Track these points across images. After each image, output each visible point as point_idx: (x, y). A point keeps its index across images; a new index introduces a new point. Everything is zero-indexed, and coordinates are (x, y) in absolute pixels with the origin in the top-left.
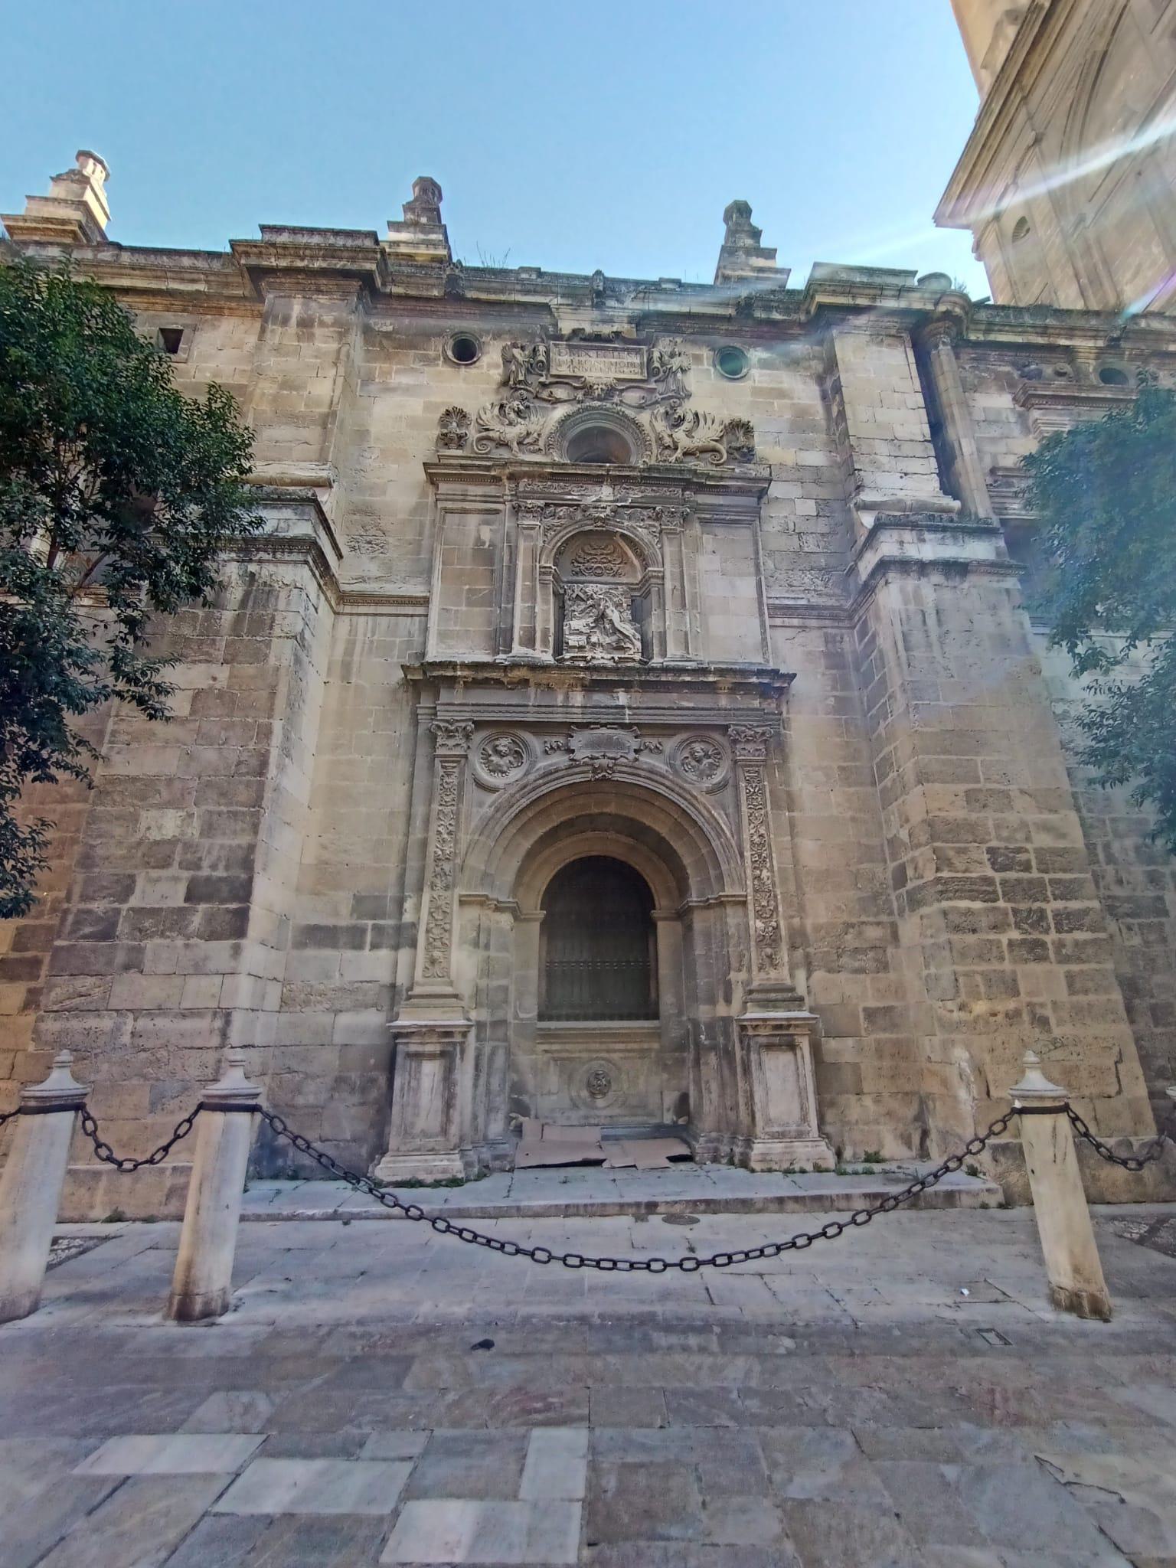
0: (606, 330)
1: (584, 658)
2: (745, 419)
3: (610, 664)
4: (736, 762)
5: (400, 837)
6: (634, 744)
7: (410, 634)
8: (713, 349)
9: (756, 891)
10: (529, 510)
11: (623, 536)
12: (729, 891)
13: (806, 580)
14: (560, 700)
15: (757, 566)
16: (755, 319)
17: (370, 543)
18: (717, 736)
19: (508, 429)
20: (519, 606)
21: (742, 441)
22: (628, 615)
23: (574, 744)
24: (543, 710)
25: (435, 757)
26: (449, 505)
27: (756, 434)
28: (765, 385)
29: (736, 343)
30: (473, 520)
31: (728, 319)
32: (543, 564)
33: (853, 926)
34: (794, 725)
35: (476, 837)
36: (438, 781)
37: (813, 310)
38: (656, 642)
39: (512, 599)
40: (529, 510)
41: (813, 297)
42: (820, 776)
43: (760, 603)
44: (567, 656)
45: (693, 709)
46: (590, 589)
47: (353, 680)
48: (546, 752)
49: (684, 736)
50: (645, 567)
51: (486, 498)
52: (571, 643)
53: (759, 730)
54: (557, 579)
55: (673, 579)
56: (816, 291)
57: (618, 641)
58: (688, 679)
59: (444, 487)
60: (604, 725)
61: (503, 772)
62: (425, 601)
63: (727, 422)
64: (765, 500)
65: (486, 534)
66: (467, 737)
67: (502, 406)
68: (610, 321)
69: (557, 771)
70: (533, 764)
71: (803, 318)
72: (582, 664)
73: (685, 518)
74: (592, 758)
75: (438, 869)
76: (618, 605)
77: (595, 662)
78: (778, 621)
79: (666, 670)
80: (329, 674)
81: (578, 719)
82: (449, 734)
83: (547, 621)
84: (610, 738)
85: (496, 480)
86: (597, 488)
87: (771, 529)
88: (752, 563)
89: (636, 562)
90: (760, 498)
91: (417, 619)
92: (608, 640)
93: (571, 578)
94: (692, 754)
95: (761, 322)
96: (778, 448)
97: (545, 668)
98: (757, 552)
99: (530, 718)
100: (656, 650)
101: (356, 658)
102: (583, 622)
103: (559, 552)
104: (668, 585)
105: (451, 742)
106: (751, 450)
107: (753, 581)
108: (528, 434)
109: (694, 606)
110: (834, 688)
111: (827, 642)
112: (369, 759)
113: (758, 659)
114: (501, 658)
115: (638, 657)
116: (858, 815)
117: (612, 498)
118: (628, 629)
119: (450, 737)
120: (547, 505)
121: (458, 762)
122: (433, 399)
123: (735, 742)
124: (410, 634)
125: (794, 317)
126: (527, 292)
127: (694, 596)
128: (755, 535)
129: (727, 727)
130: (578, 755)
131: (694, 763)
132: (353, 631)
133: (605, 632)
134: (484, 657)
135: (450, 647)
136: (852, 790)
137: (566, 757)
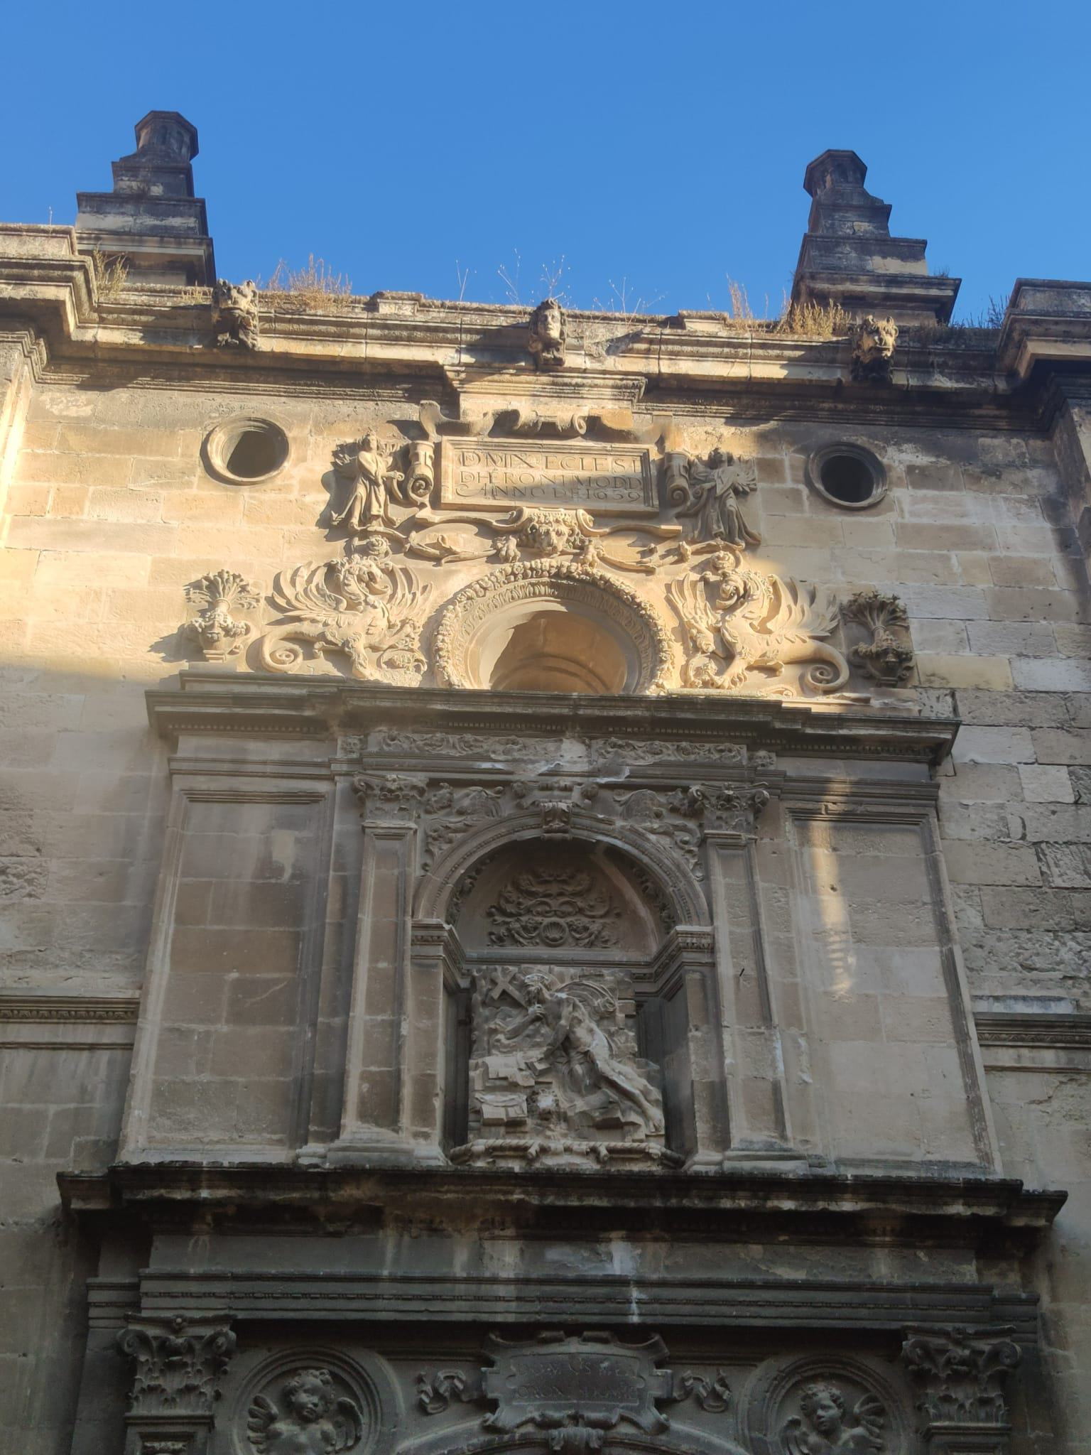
0: (564, 412)
1: (521, 1152)
2: (886, 593)
3: (588, 1166)
4: (928, 1436)
6: (654, 1381)
7: (83, 1093)
8: (804, 450)
10: (390, 796)
11: (614, 853)
13: (1065, 954)
14: (460, 1263)
15: (942, 923)
16: (899, 388)
18: (874, 1363)
19: (346, 618)
20: (360, 1015)
21: (883, 638)
22: (628, 1039)
23: (497, 1382)
24: (416, 1289)
25: (127, 1423)
26: (202, 783)
27: (914, 624)
28: (925, 520)
29: (858, 437)
30: (255, 819)
31: (835, 391)
32: (422, 917)
34: (1074, 1332)
37: (1023, 370)
38: (701, 1109)
39: (344, 1005)
40: (390, 796)
41: (1021, 346)
43: (957, 1011)
44: (479, 1145)
46: (535, 977)
48: (422, 1409)
49: (785, 1362)
50: (667, 922)
51: (288, 770)
52: (489, 1112)
53: (985, 1346)
54: (455, 955)
55: (735, 954)
56: (1026, 334)
57: (608, 1106)
58: (788, 1205)
59: (189, 746)
60: (575, 1330)
62: (129, 1012)
63: (845, 599)
64: (946, 767)
65: (286, 849)
66: (216, 1366)
67: (331, 570)
68: (574, 391)
71: (1002, 385)
72: (517, 1166)
73: (758, 809)
74: (546, 1424)
76: (604, 1017)
77: (550, 1162)
78: (1006, 1057)
81: (506, 1313)
82: (170, 1360)
83: (429, 1056)
84: (592, 1364)
85: (314, 729)
86: (551, 746)
87: (966, 834)
88: (927, 915)
89: (643, 912)
90: (935, 763)
91: (104, 1056)
92: (581, 1104)
93: (486, 951)
95: (906, 395)
96: (967, 653)
97: (426, 1177)
98: (936, 887)
99: (385, 1311)
100: (702, 1128)
102: (518, 1058)
103: (461, 891)
104: (726, 968)
105: (171, 1383)
106: (904, 658)
107: (931, 958)
109: (794, 1019)
113: (965, 1153)
114: (312, 1153)
115: (656, 1147)
117: (585, 767)
118: (630, 1076)
119: (171, 1367)
120: (434, 784)
121: (188, 1438)
122: (173, 555)
123: (922, 1378)
124: (83, 1093)
125: (985, 383)
126: (396, 341)
128: (929, 848)
129: (897, 1337)
130: (506, 1416)
131: (813, 1438)
133: (574, 1084)
134: (277, 1155)
135: (185, 1126)
137: (475, 1423)
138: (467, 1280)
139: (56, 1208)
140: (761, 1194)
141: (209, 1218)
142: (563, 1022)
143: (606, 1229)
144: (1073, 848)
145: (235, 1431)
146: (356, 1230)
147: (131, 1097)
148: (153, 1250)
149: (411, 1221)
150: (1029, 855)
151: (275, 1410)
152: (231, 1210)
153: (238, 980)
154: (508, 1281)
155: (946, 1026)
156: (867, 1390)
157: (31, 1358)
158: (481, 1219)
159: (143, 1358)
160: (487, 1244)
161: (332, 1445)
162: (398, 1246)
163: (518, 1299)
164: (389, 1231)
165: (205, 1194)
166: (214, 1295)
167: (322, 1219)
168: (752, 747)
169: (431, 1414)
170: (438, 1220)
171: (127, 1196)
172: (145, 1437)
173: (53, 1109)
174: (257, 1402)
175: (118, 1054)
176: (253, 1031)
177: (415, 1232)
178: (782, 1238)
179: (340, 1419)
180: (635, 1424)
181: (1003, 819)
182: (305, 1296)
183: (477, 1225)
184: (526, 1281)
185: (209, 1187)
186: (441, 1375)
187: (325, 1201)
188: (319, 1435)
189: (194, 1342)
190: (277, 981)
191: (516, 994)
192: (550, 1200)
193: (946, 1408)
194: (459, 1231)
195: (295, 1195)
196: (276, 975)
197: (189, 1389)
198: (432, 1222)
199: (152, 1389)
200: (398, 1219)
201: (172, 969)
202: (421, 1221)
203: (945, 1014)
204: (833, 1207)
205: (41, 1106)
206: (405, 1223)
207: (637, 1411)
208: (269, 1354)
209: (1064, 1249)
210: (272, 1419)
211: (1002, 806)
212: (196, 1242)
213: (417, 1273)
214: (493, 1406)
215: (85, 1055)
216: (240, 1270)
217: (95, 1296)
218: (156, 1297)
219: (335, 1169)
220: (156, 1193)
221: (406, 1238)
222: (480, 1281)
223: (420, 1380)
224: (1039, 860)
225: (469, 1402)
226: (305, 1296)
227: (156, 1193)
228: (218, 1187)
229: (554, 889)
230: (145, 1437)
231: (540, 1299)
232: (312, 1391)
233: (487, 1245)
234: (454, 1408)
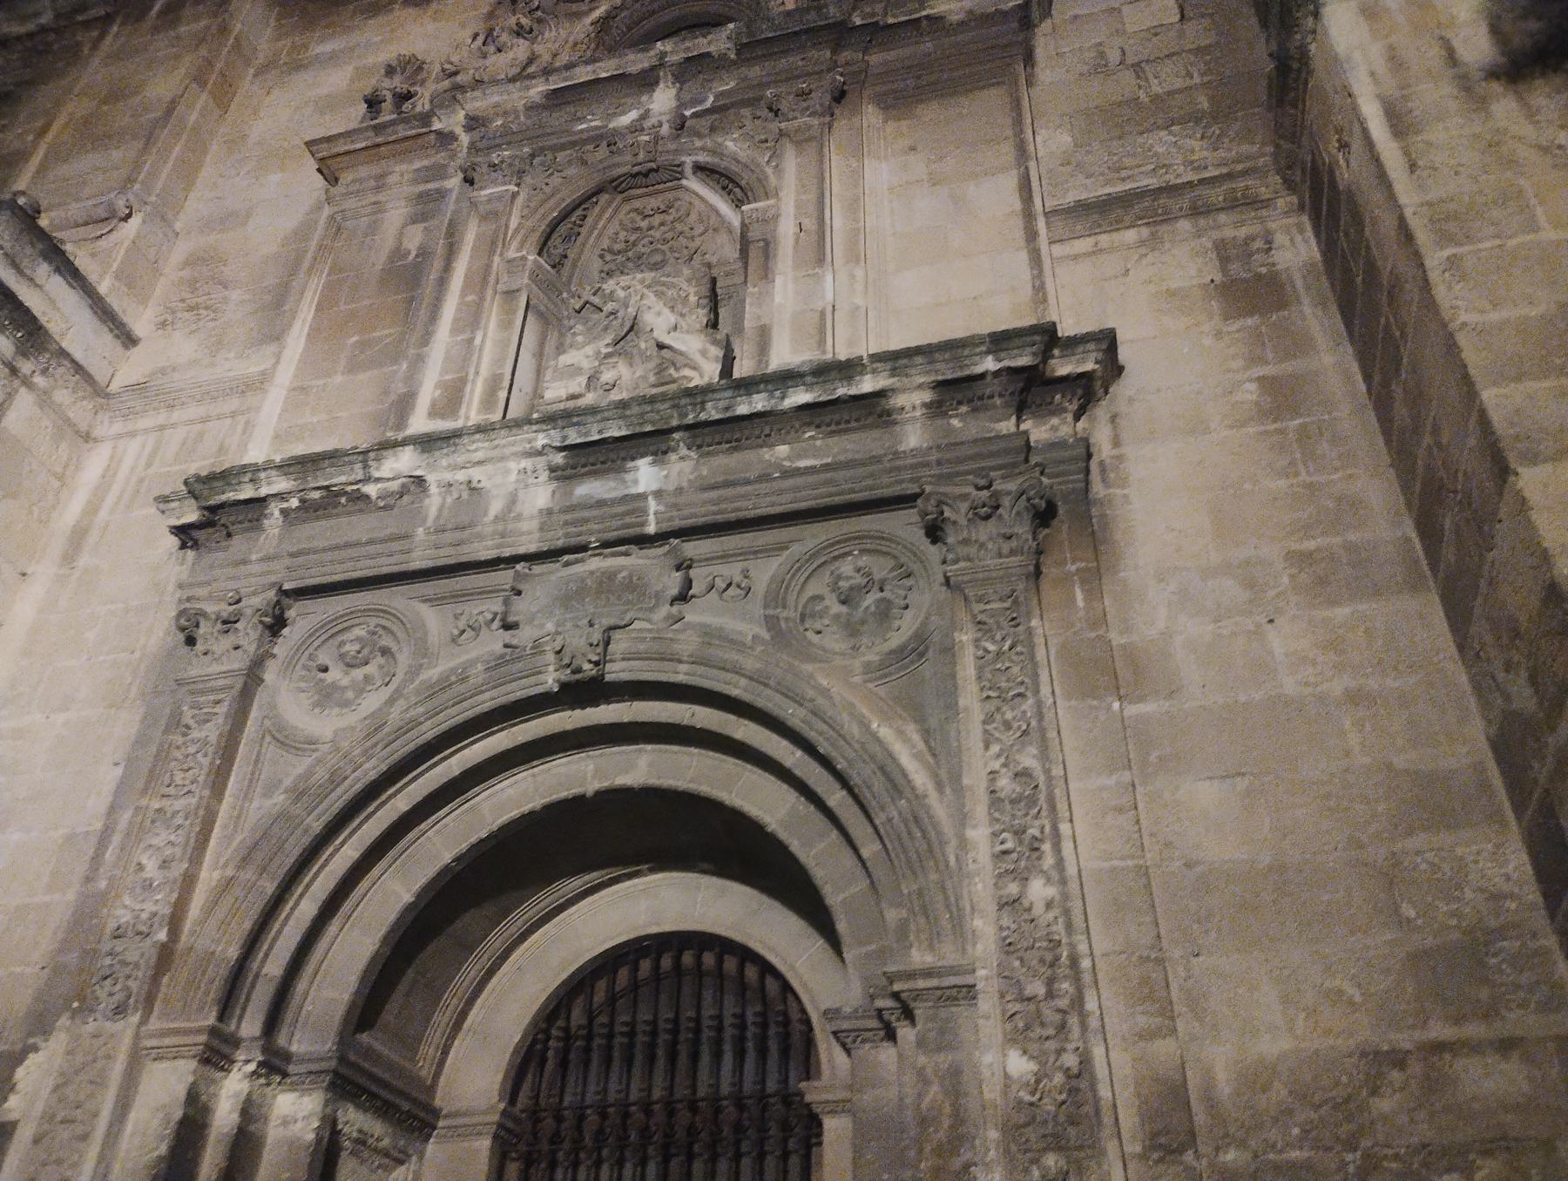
9: (1008, 947)
12: (920, 957)
17: (191, 309)
33: (1398, 1059)
42: (1230, 590)
45: (826, 468)
61: (345, 704)
70: (414, 672)
79: (747, 386)
84: (610, 575)
94: (834, 588)
101: (103, 514)
102: (589, 350)
108: (530, 61)
110: (1255, 360)
111: (1224, 260)
116: (1373, 684)
127: (855, 237)
136: (1342, 612)
140: (778, 393)
141: (277, 513)
142: (629, 310)
143: (633, 459)
144: (1174, 58)
150: (1128, 77)
153: (357, 342)
155: (1019, 234)
156: (895, 557)
157: (137, 655)
168: (837, 48)
172: (192, 693)
176: (362, 377)
178: (807, 435)
180: (649, 621)
181: (1102, 55)
190: (391, 335)
191: (596, 300)
192: (574, 437)
193: (963, 551)
196: (386, 332)
201: (306, 345)
203: (1018, 223)
204: (853, 391)
207: (651, 610)
209: (1131, 400)
211: (1100, 44)
224: (1138, 77)
229: (657, 219)
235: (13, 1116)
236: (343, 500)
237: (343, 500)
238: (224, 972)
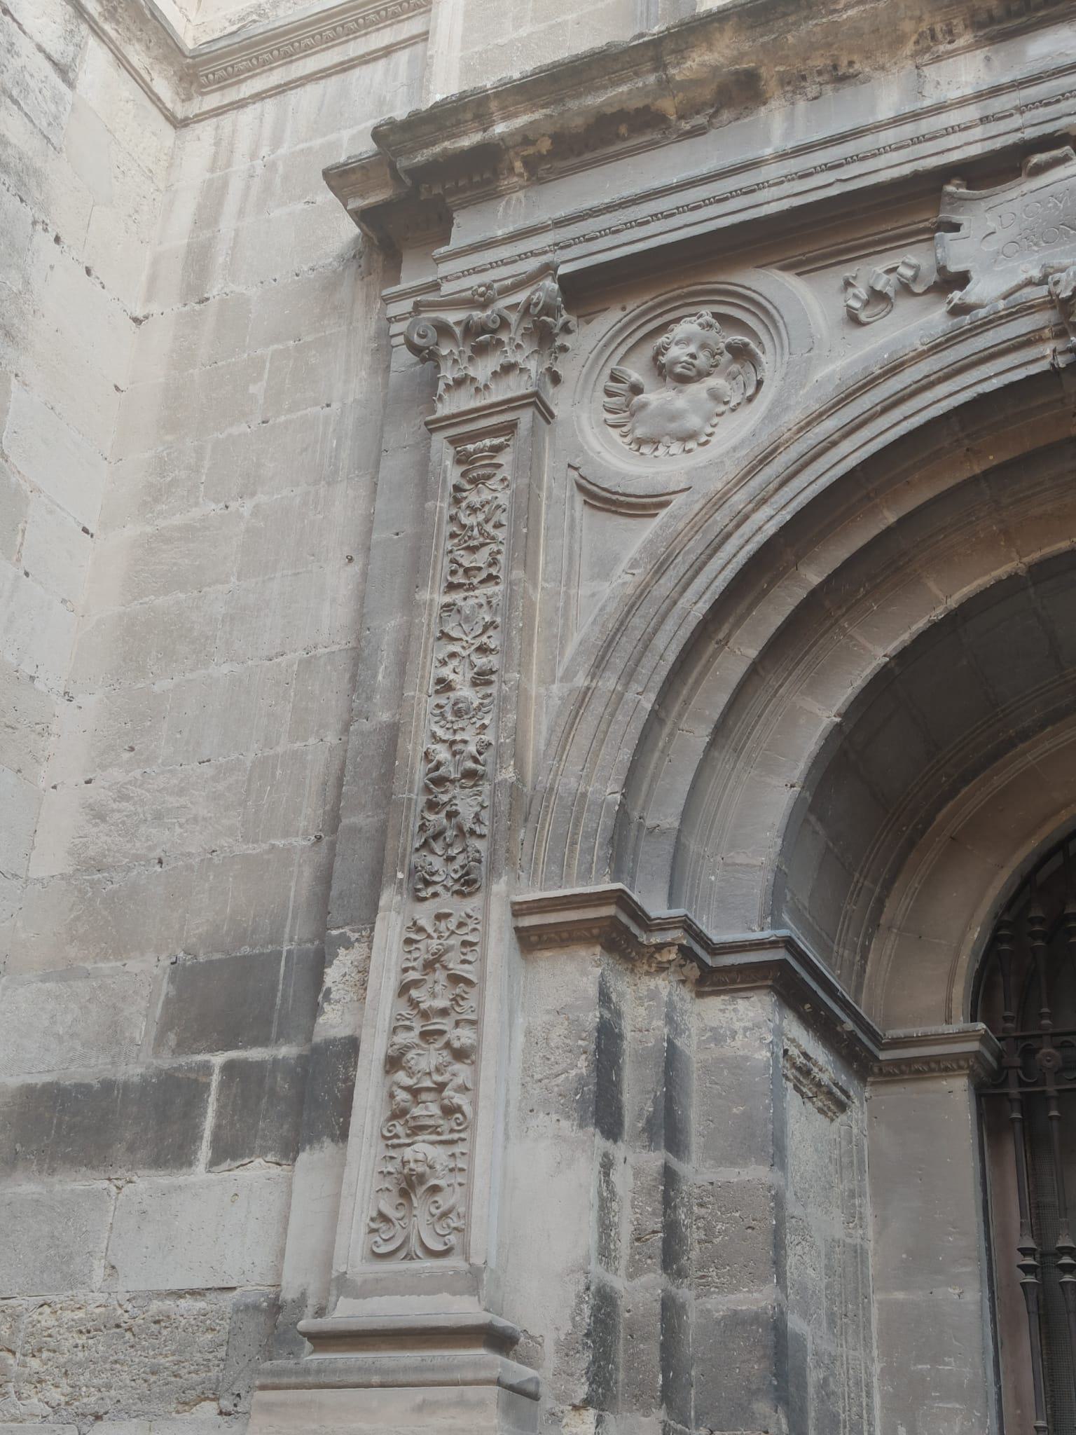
5: (331, 738)
35: (581, 681)
36: (443, 505)
47: (215, 290)
48: (854, 319)
69: (894, 369)
75: (437, 819)
80: (149, 298)
91: (403, 57)
99: (772, 202)
101: (227, 225)
105: (483, 369)
112: (247, 508)
119: (481, 350)
132: (220, 161)
138: (898, 121)
139: (356, 240)
141: (518, 165)
145: (584, 417)
146: (726, 115)
147: (429, 81)
148: (454, 230)
149: (804, 78)
151: (635, 376)
152: (545, 145)
154: (963, 102)
158: (914, 38)
159: (444, 352)
160: (927, 71)
161: (726, 403)
162: (790, 118)
163: (984, 120)
164: (773, 104)
165: (500, 128)
166: (533, 254)
167: (673, 118)
169: (868, 323)
170: (844, 62)
171: (403, 163)
173: (346, 134)
174: (614, 378)
175: (419, 47)
177: (812, 90)
179: (735, 367)
182: (655, 217)
183: (909, 48)
184: (996, 91)
185: (504, 119)
186: (880, 269)
187: (665, 85)
188: (704, 395)
189: (506, 313)
194: (883, 68)
195: (624, 88)
197: (508, 369)
198: (835, 67)
199: (459, 383)
200: (784, 81)
202: (820, 73)
205: (332, 137)
206: (794, 82)
208: (625, 313)
210: (636, 389)
212: (508, 202)
213: (816, 137)
214: (962, 280)
215: (381, 64)
216: (561, 213)
217: (396, 309)
218: (459, 278)
219: (668, 29)
220: (437, 149)
221: (802, 105)
222: (915, 116)
223: (848, 284)
225: (925, 293)
226: (655, 217)
227: (437, 149)
228: (515, 115)
230: (454, 441)
231: (1021, 110)
232: (687, 341)
233: (930, 72)
234: (904, 306)
235: (343, 1032)
236: (623, 130)
237: (623, 130)
238: (605, 822)
